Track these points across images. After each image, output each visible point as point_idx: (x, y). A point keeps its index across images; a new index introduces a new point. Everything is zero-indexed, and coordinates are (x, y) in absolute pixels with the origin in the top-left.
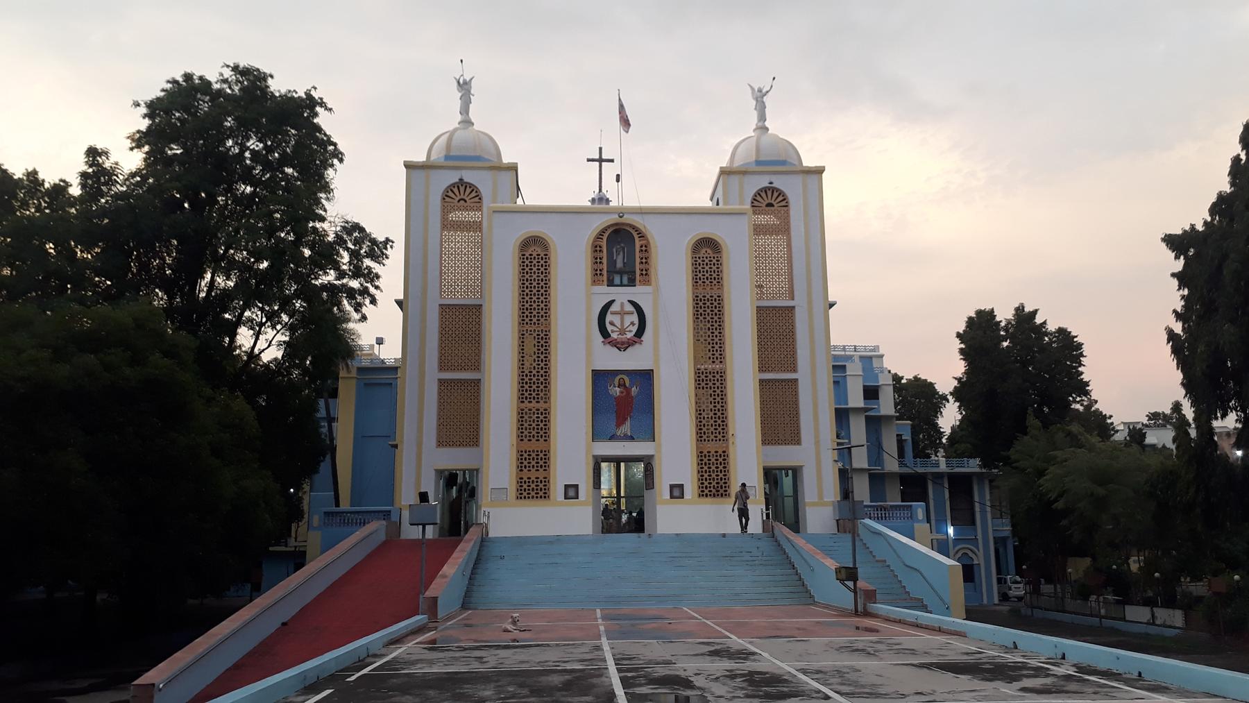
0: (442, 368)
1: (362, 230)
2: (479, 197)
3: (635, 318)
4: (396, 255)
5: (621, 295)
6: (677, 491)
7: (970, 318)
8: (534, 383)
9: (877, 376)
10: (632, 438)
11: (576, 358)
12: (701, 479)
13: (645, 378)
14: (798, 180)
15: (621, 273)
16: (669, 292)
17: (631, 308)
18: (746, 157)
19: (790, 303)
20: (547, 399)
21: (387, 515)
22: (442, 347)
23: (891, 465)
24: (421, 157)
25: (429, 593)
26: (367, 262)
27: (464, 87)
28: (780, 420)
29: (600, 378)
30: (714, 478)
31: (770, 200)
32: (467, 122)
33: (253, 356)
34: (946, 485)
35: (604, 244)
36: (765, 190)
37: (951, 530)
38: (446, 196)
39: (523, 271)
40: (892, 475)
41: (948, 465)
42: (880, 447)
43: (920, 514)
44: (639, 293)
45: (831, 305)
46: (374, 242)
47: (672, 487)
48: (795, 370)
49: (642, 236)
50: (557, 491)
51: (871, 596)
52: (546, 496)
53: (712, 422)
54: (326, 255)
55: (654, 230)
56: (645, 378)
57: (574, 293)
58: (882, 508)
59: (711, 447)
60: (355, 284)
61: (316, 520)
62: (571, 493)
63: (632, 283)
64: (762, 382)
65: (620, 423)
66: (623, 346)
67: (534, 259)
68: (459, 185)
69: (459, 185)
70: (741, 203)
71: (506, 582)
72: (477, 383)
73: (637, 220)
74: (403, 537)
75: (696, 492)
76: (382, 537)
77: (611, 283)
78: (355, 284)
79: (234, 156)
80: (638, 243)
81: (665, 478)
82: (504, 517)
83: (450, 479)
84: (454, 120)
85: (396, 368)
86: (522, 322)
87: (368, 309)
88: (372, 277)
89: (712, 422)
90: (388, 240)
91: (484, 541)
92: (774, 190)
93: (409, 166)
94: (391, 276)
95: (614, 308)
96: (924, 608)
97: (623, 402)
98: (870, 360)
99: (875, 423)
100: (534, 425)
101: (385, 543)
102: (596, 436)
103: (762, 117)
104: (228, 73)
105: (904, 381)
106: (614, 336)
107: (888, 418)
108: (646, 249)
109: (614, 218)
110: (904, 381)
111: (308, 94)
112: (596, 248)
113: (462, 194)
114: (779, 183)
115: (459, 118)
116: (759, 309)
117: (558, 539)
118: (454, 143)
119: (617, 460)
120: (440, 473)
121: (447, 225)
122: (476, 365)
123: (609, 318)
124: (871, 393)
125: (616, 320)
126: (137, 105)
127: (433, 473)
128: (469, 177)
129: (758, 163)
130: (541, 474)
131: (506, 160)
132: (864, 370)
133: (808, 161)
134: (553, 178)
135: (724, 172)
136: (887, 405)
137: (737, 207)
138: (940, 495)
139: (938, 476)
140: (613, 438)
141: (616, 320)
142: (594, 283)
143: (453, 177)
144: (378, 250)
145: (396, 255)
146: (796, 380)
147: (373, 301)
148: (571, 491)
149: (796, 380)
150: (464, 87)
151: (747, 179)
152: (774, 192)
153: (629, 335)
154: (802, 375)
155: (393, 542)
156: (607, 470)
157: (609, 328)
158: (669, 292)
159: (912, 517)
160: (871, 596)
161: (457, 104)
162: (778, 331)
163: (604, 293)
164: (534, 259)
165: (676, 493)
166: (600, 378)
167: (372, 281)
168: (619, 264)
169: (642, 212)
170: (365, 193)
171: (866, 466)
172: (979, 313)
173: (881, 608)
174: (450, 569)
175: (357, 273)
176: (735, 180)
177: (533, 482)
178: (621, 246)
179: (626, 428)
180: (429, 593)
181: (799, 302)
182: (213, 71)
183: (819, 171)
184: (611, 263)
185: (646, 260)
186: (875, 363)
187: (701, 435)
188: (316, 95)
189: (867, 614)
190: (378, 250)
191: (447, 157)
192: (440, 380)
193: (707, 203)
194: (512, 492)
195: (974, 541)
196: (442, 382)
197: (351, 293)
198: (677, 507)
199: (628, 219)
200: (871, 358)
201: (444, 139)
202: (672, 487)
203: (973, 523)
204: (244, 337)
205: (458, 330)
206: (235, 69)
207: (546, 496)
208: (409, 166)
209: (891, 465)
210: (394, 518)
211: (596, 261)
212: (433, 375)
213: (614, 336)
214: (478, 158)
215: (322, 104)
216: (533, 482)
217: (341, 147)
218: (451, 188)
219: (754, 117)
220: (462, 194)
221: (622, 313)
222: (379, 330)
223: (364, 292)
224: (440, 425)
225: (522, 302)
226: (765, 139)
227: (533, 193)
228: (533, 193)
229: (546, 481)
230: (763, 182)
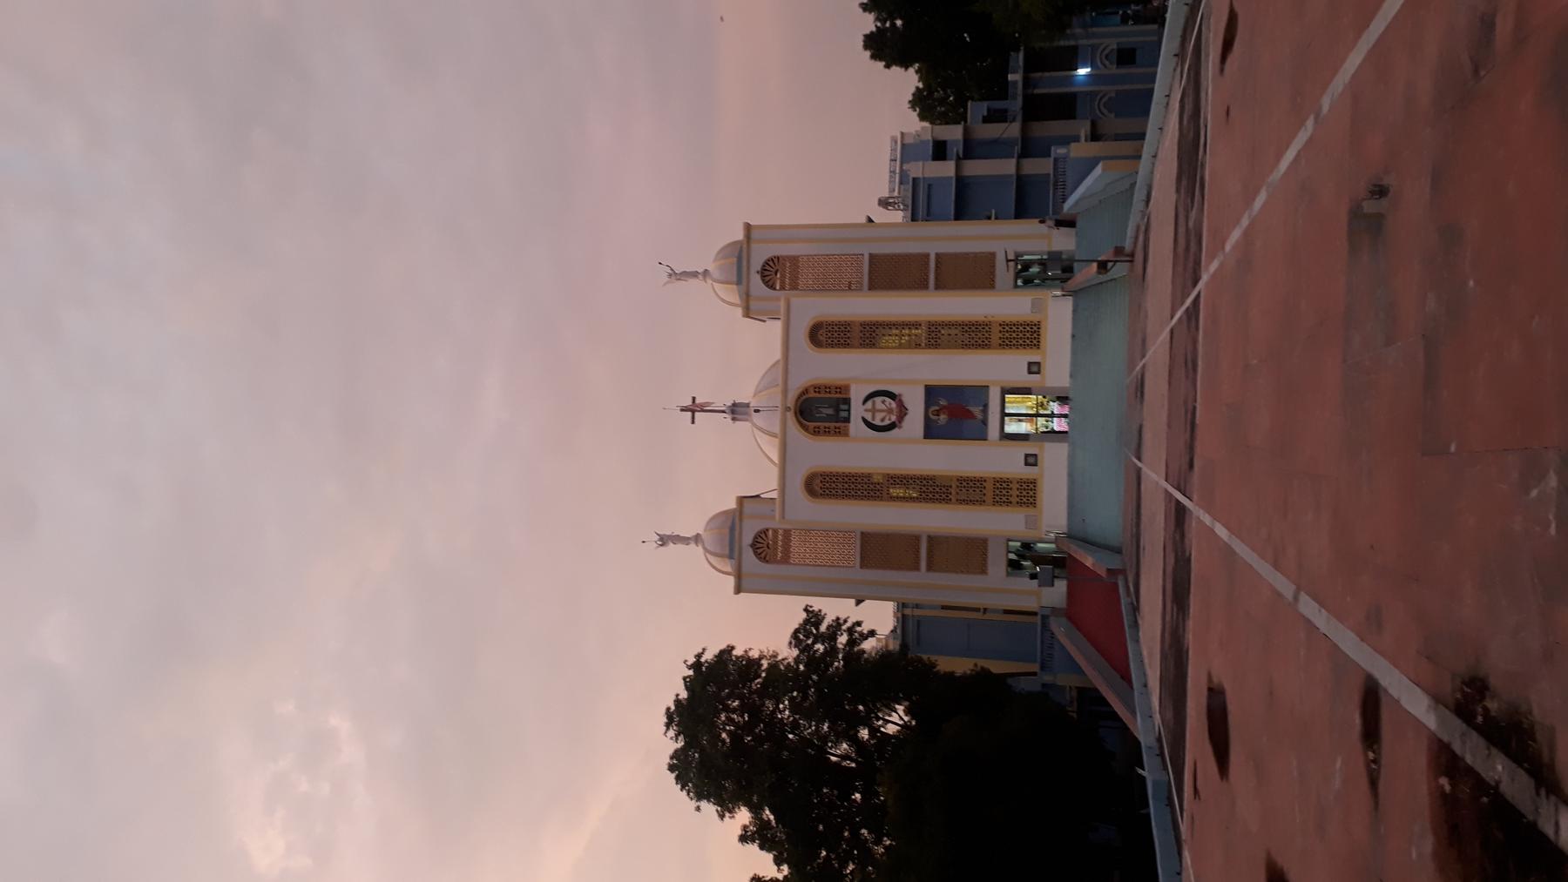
0: (917, 568)
1: (797, 631)
2: (765, 531)
3: (878, 400)
4: (817, 603)
5: (857, 410)
6: (1034, 368)
7: (873, 57)
8: (932, 489)
9: (923, 142)
10: (986, 406)
11: (912, 452)
12: (1024, 346)
13: (932, 392)
14: (754, 246)
15: (838, 410)
16: (854, 369)
17: (869, 403)
18: (731, 294)
19: (867, 257)
20: (950, 478)
21: (1044, 618)
22: (899, 568)
23: (1013, 130)
24: (730, 581)
25: (1103, 574)
26: (823, 628)
27: (664, 540)
28: (972, 273)
29: (931, 432)
30: (1025, 335)
31: (772, 271)
32: (697, 539)
33: (905, 726)
34: (1039, 74)
35: (812, 425)
36: (763, 277)
37: (1083, 71)
38: (764, 560)
39: (836, 496)
40: (1024, 129)
41: (1015, 72)
42: (995, 142)
43: (1061, 151)
44: (857, 394)
45: (870, 220)
46: (806, 622)
47: (1030, 372)
48: (927, 256)
49: (806, 391)
50: (1030, 472)
51: (1119, 251)
52: (1034, 482)
53: (974, 335)
54: (815, 663)
55: (798, 382)
56: (932, 392)
57: (856, 452)
58: (1055, 185)
59: (995, 337)
60: (843, 639)
61: (1047, 678)
62: (1031, 460)
63: (847, 401)
64: (938, 287)
65: (970, 415)
66: (902, 411)
67: (824, 485)
68: (755, 547)
69: (755, 547)
70: (778, 299)
71: (1107, 519)
72: (931, 539)
73: (792, 395)
74: (1064, 605)
75: (1035, 351)
76: (1064, 620)
77: (847, 420)
78: (843, 639)
79: (731, 734)
80: (812, 395)
81: (1022, 378)
82: (1051, 518)
83: (1014, 566)
84: (696, 551)
85: (904, 616)
86: (881, 498)
87: (865, 628)
88: (837, 624)
89: (974, 335)
90: (806, 610)
91: (1070, 536)
92: (764, 269)
93: (738, 590)
94: (834, 608)
95: (869, 418)
96: (1133, 185)
97: (956, 413)
98: (907, 151)
99: (971, 149)
100: (969, 490)
101: (1070, 618)
102: (983, 437)
103: (695, 274)
104: (671, 733)
105: (921, 85)
106: (894, 418)
107: (966, 130)
108: (817, 388)
109: (790, 416)
110: (921, 85)
111: (690, 667)
112: (816, 432)
113: (764, 547)
114: (757, 264)
115: (693, 545)
116: (872, 287)
117: (1070, 475)
118: (718, 551)
119: (1004, 415)
120: (1008, 574)
121: (786, 560)
122: (914, 539)
123: (877, 422)
124: (940, 151)
125: (879, 416)
126: (698, 809)
127: (1012, 580)
128: (748, 538)
129: (739, 283)
130: (1015, 486)
131: (733, 505)
132: (916, 160)
133: (740, 235)
134: (747, 464)
135: (747, 313)
136: (953, 133)
137: (782, 304)
138: (1047, 129)
139: (1026, 80)
140: (985, 422)
141: (879, 416)
142: (847, 435)
143: (749, 555)
144: (814, 618)
145: (817, 603)
146: (938, 256)
147: (859, 624)
148: (1031, 460)
149: (938, 256)
150: (664, 540)
151: (753, 292)
152: (767, 270)
153: (894, 405)
154: (932, 249)
155: (1071, 613)
156: (1012, 427)
157: (887, 422)
158: (854, 369)
159: (1065, 158)
160: (1119, 251)
161: (680, 547)
162: (890, 272)
163: (856, 426)
164: (824, 485)
165: (1035, 369)
166: (931, 432)
167: (839, 625)
168: (830, 411)
169: (785, 392)
170: (765, 628)
171: (1013, 161)
172: (866, 47)
173: (1128, 246)
174: (1089, 561)
175: (831, 635)
176: (753, 304)
177: (1023, 493)
178: (819, 410)
179: (977, 411)
180: (1103, 574)
181: (866, 250)
182: (669, 744)
183: (748, 227)
184: (829, 418)
185: (827, 388)
186: (908, 140)
187: (984, 345)
188: (692, 660)
189: (1132, 255)
190: (814, 618)
191: (731, 557)
192: (930, 568)
193: (777, 327)
194: (1031, 511)
195: (1094, 48)
196: (930, 568)
197: (852, 642)
198: (1048, 368)
199: (791, 403)
200: (903, 145)
201: (712, 559)
202: (1030, 372)
203: (1075, 49)
204: (891, 729)
205: (881, 552)
206: (668, 726)
207: (1034, 482)
208: (738, 590)
209: (1013, 130)
210: (1047, 612)
211: (827, 432)
212: (922, 576)
213: (894, 418)
214: (732, 529)
215: (699, 656)
216: (1023, 493)
217: (723, 646)
218: (758, 555)
219: (693, 282)
220: (764, 547)
221: (874, 411)
222: (878, 620)
223: (850, 631)
224: (967, 569)
225: (862, 498)
226: (716, 274)
227: (766, 483)
228: (766, 483)
229: (1021, 482)
230: (756, 279)
